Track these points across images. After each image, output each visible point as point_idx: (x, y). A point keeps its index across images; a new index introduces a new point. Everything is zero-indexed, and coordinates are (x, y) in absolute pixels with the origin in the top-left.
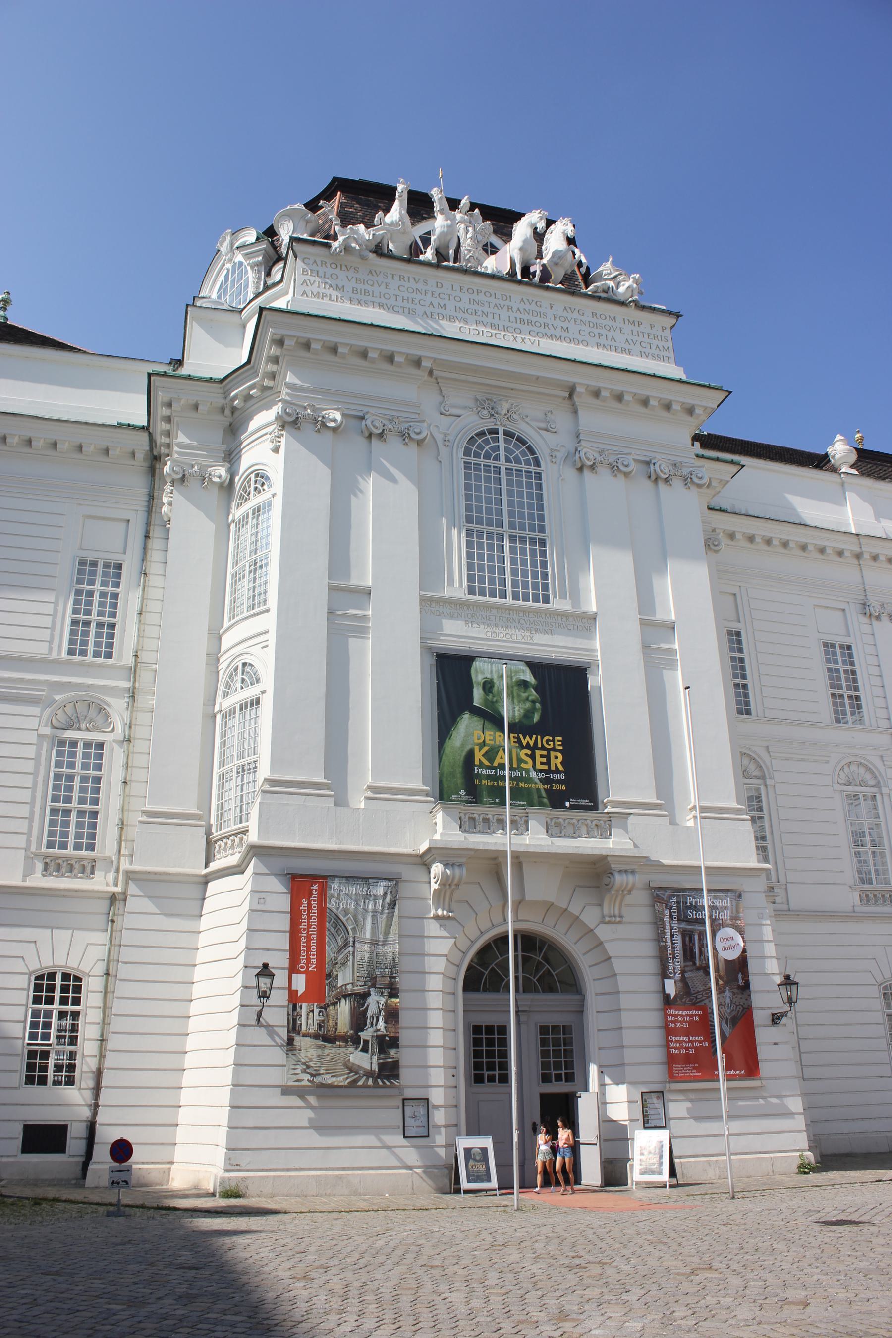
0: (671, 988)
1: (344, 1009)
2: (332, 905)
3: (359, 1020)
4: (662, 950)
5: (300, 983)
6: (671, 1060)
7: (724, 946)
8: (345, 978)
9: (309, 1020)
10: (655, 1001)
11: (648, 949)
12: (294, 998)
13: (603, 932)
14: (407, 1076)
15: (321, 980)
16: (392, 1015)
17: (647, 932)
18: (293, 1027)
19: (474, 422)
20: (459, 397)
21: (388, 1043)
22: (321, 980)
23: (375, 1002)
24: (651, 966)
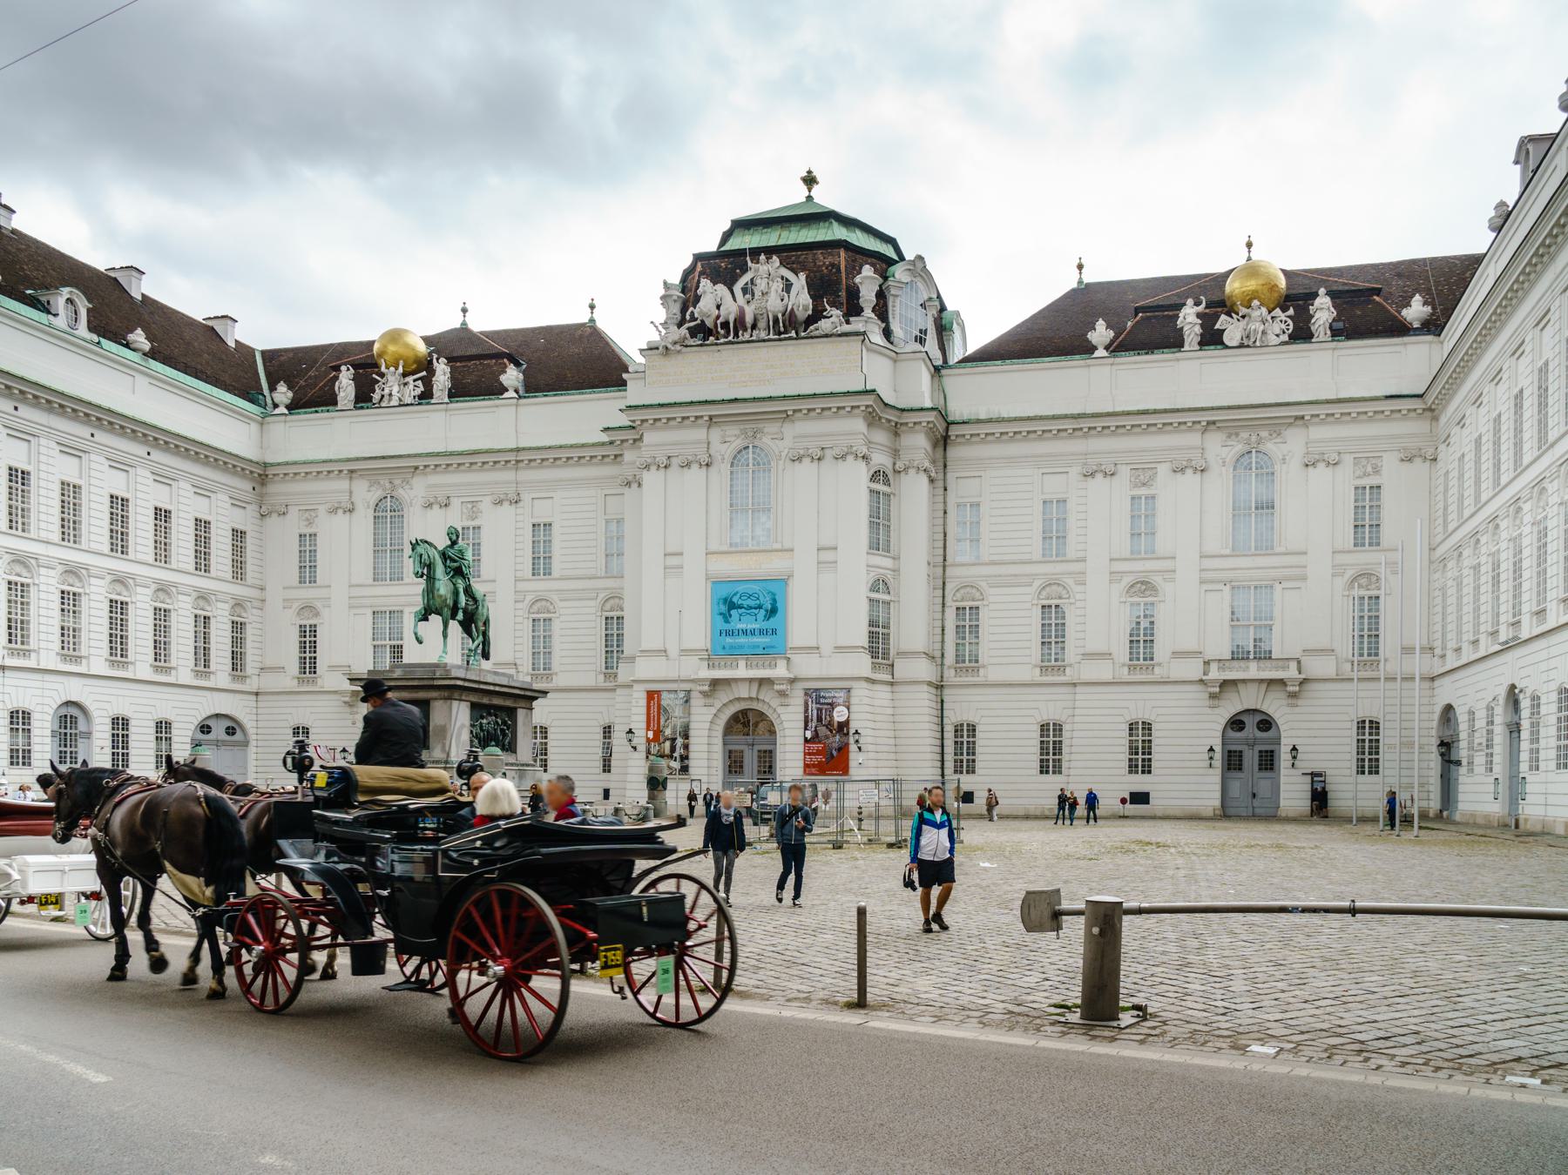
0: (809, 734)
1: (668, 744)
2: (663, 703)
3: (673, 749)
4: (806, 718)
5: (651, 735)
6: (806, 766)
7: (840, 715)
8: (668, 732)
9: (654, 749)
10: (802, 740)
11: (802, 717)
12: (649, 741)
13: (780, 710)
14: (691, 770)
15: (658, 733)
16: (686, 747)
17: (802, 709)
18: (648, 752)
19: (738, 443)
20: (732, 430)
21: (684, 758)
22: (658, 733)
23: (679, 741)
24: (802, 725)
